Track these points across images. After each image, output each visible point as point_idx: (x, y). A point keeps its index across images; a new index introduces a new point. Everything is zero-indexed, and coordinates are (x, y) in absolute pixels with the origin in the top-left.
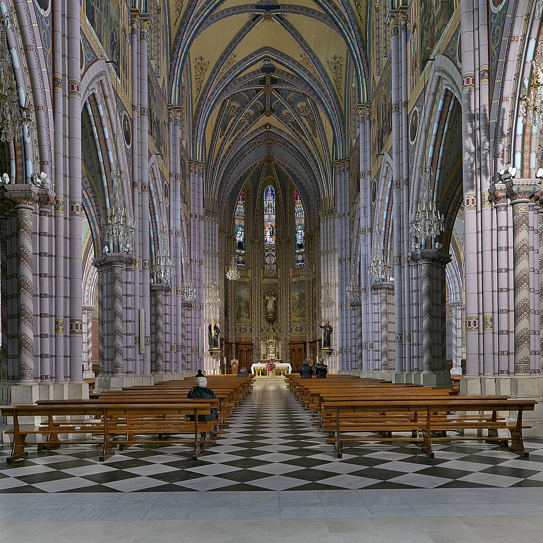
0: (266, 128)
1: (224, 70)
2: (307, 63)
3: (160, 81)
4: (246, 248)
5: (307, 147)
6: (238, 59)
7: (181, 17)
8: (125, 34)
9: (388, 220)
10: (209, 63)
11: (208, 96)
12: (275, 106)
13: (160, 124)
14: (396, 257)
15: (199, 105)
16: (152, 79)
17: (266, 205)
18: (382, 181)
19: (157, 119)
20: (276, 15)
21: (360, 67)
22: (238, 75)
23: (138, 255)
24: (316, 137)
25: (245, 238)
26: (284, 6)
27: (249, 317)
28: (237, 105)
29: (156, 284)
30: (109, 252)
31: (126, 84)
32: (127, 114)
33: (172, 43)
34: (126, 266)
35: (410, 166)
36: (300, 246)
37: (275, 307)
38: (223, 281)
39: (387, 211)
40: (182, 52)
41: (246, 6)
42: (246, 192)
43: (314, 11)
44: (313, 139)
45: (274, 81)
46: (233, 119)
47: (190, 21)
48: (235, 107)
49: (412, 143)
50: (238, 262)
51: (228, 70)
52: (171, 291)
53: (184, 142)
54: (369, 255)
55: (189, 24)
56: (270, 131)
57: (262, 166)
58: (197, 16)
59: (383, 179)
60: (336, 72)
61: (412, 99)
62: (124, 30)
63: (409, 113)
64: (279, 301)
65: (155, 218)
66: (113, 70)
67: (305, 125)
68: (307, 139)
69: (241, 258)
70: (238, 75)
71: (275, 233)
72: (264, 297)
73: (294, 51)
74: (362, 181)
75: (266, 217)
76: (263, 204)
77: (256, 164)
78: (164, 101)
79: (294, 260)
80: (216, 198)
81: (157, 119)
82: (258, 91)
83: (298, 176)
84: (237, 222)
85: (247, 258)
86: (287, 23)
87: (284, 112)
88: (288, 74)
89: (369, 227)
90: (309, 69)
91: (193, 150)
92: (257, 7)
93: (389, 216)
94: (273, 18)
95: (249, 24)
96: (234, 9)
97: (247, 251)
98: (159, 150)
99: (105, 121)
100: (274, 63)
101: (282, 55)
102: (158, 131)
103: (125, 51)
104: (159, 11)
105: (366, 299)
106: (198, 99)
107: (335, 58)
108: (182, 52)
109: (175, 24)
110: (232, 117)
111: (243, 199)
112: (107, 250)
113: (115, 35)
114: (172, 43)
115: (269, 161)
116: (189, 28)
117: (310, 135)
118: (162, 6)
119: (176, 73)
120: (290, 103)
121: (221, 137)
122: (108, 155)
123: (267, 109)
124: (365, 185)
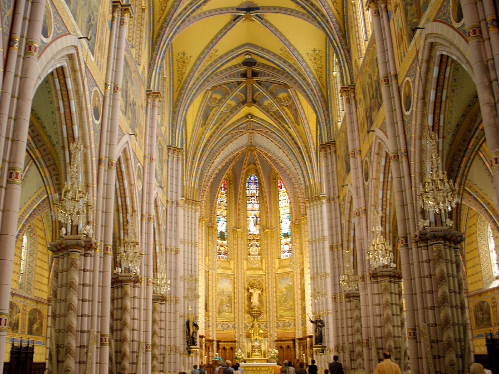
0: (248, 118)
1: (206, 62)
2: (287, 56)
3: (140, 69)
4: (228, 238)
5: (290, 135)
6: (220, 54)
7: (164, 15)
8: (105, 20)
9: (385, 199)
10: (191, 57)
11: (190, 86)
12: (256, 97)
13: (137, 106)
14: (401, 237)
15: (180, 94)
16: (132, 64)
17: (248, 194)
18: (374, 158)
19: (133, 101)
20: (256, 15)
21: (341, 54)
22: (219, 67)
23: (99, 239)
24: (299, 125)
25: (227, 228)
26: (263, 8)
27: (231, 312)
28: (219, 97)
29: (123, 274)
30: (66, 234)
31: (101, 62)
32: (98, 90)
33: (155, 37)
34: (85, 251)
35: (408, 136)
36: (286, 236)
37: (260, 301)
38: (204, 274)
39: (383, 190)
40: (164, 44)
41: (227, 9)
43: (292, 11)
44: (295, 127)
45: (255, 74)
46: (214, 109)
47: (174, 18)
48: (216, 98)
49: (407, 113)
50: (220, 254)
51: (209, 63)
52: (141, 283)
53: (163, 129)
54: (365, 240)
55: (172, 21)
56: (252, 121)
57: (244, 154)
58: (180, 15)
59: (376, 156)
60: (316, 63)
61: (402, 71)
62: (104, 17)
63: (399, 84)
64: (264, 294)
65: (125, 201)
66: (86, 47)
67: (287, 114)
68: (289, 128)
69: (222, 249)
70: (219, 67)
71: (258, 222)
72: (248, 290)
73: (275, 46)
74: (351, 160)
75: (249, 206)
76: (246, 193)
77: (238, 154)
78: (142, 86)
80: (196, 186)
81: (133, 101)
82: (239, 83)
83: (282, 165)
84: (218, 212)
86: (267, 21)
87: (266, 103)
88: (269, 67)
89: (363, 208)
90: (289, 61)
91: (172, 136)
92: (238, 9)
93: (385, 195)
94: (253, 18)
95: (230, 23)
96: (216, 10)
98: (133, 130)
99: (72, 95)
100: (255, 57)
101: (263, 49)
102: (134, 113)
103: (102, 34)
104: (143, 10)
105: (365, 288)
106: (179, 89)
107: (314, 51)
108: (164, 44)
109: (159, 21)
110: (213, 108)
112: (64, 232)
113: (92, 17)
114: (155, 37)
115: (251, 150)
116: (172, 25)
117: (293, 123)
118: (147, 6)
119: (156, 62)
120: (271, 93)
121: (202, 127)
122: (73, 130)
123: (248, 100)
124: (355, 164)
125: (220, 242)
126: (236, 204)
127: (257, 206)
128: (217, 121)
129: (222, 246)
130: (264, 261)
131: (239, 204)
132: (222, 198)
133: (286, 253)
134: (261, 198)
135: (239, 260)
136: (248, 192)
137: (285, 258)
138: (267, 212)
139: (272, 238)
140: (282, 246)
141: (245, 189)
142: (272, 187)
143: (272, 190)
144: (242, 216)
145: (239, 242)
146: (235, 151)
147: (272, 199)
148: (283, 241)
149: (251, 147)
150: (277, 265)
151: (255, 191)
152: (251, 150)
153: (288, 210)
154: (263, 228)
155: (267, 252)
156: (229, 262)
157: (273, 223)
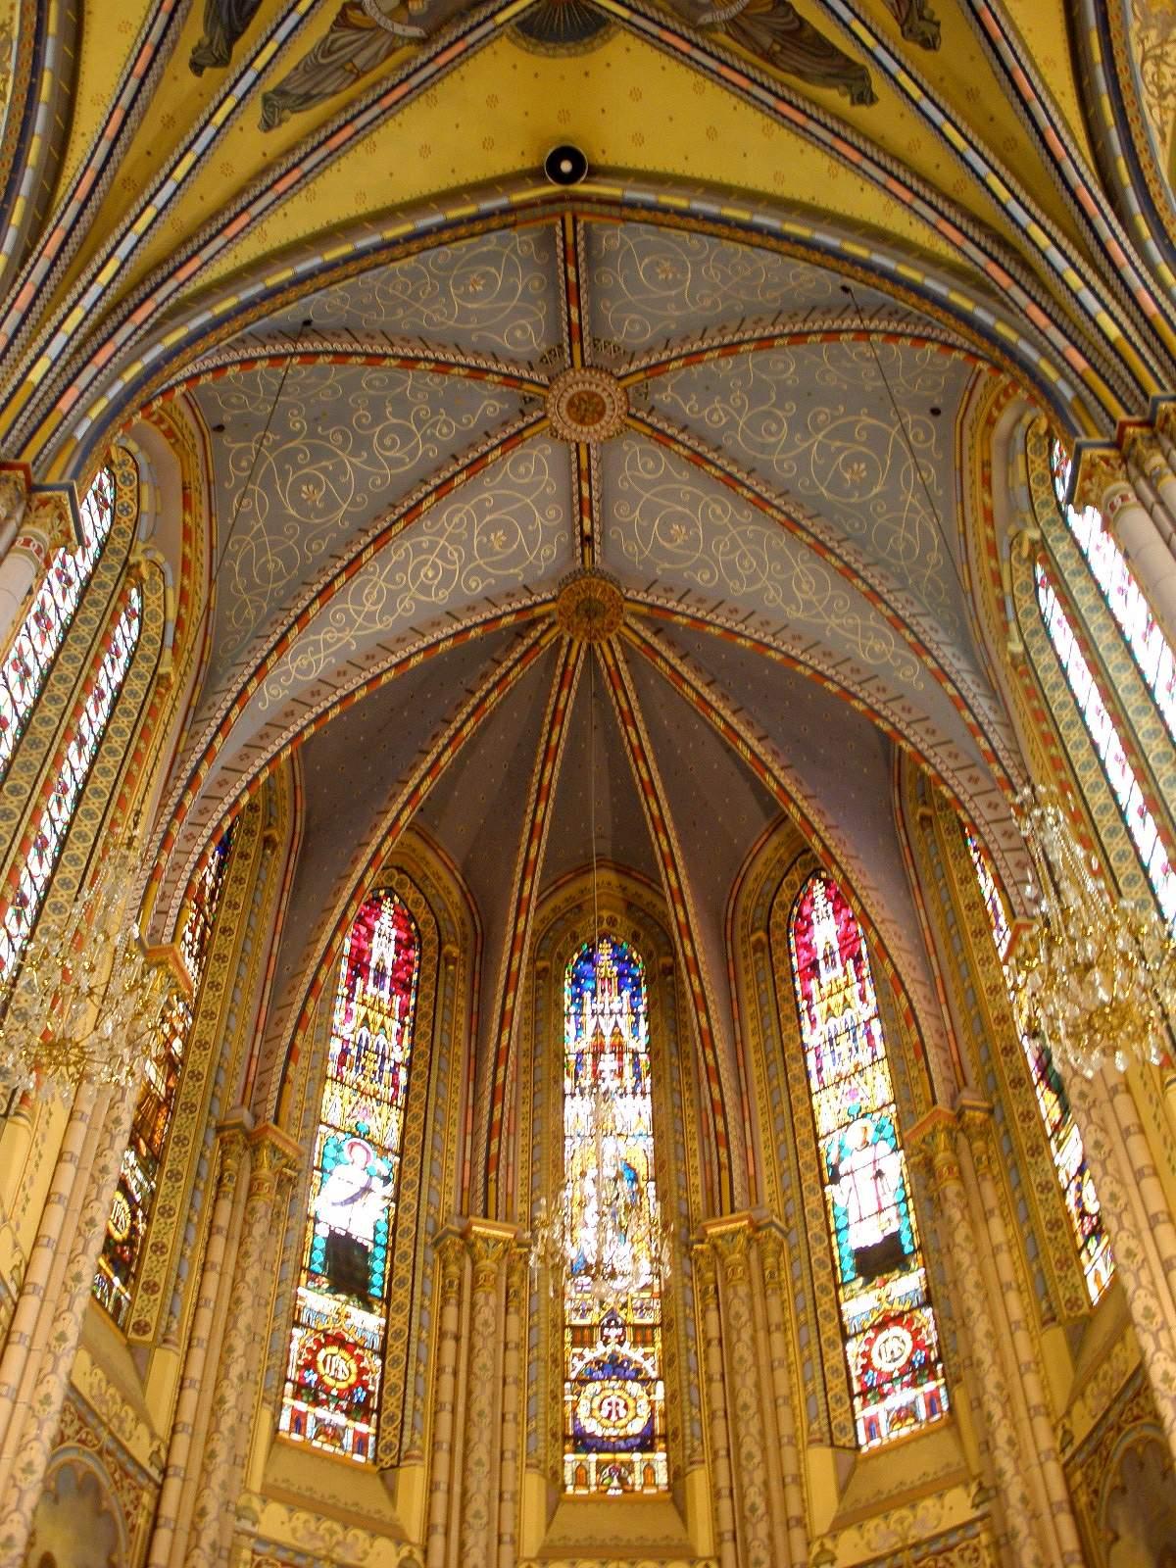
4: (400, 1295)
17: (575, 1040)
36: (881, 1260)
42: (431, 951)
75: (577, 1111)
76: (560, 1032)
79: (837, 1385)
84: (335, 1104)
85: (394, 1376)
97: (399, 1320)
111: (401, 986)
125: (319, 1301)
126: (475, 1076)
127: (635, 1112)
128: (311, 67)
129: (339, 1341)
130: (699, 1481)
131: (501, 1056)
132: (367, 1020)
133: (901, 1397)
134: (675, 1061)
135: (480, 1452)
136: (570, 1027)
137: (888, 1434)
138: (719, 1108)
139: (769, 1283)
140: (853, 1348)
141: (545, 1017)
142: (746, 979)
143: (747, 994)
144: (516, 1151)
145: (485, 1314)
146: (471, 609)
147: (752, 1042)
148: (860, 1304)
149: (588, 595)
150: (824, 1503)
151: (624, 1023)
152: (590, 610)
153: (879, 1087)
154: (682, 1232)
155: (731, 1394)
156: (386, 1475)
157: (766, 1189)
